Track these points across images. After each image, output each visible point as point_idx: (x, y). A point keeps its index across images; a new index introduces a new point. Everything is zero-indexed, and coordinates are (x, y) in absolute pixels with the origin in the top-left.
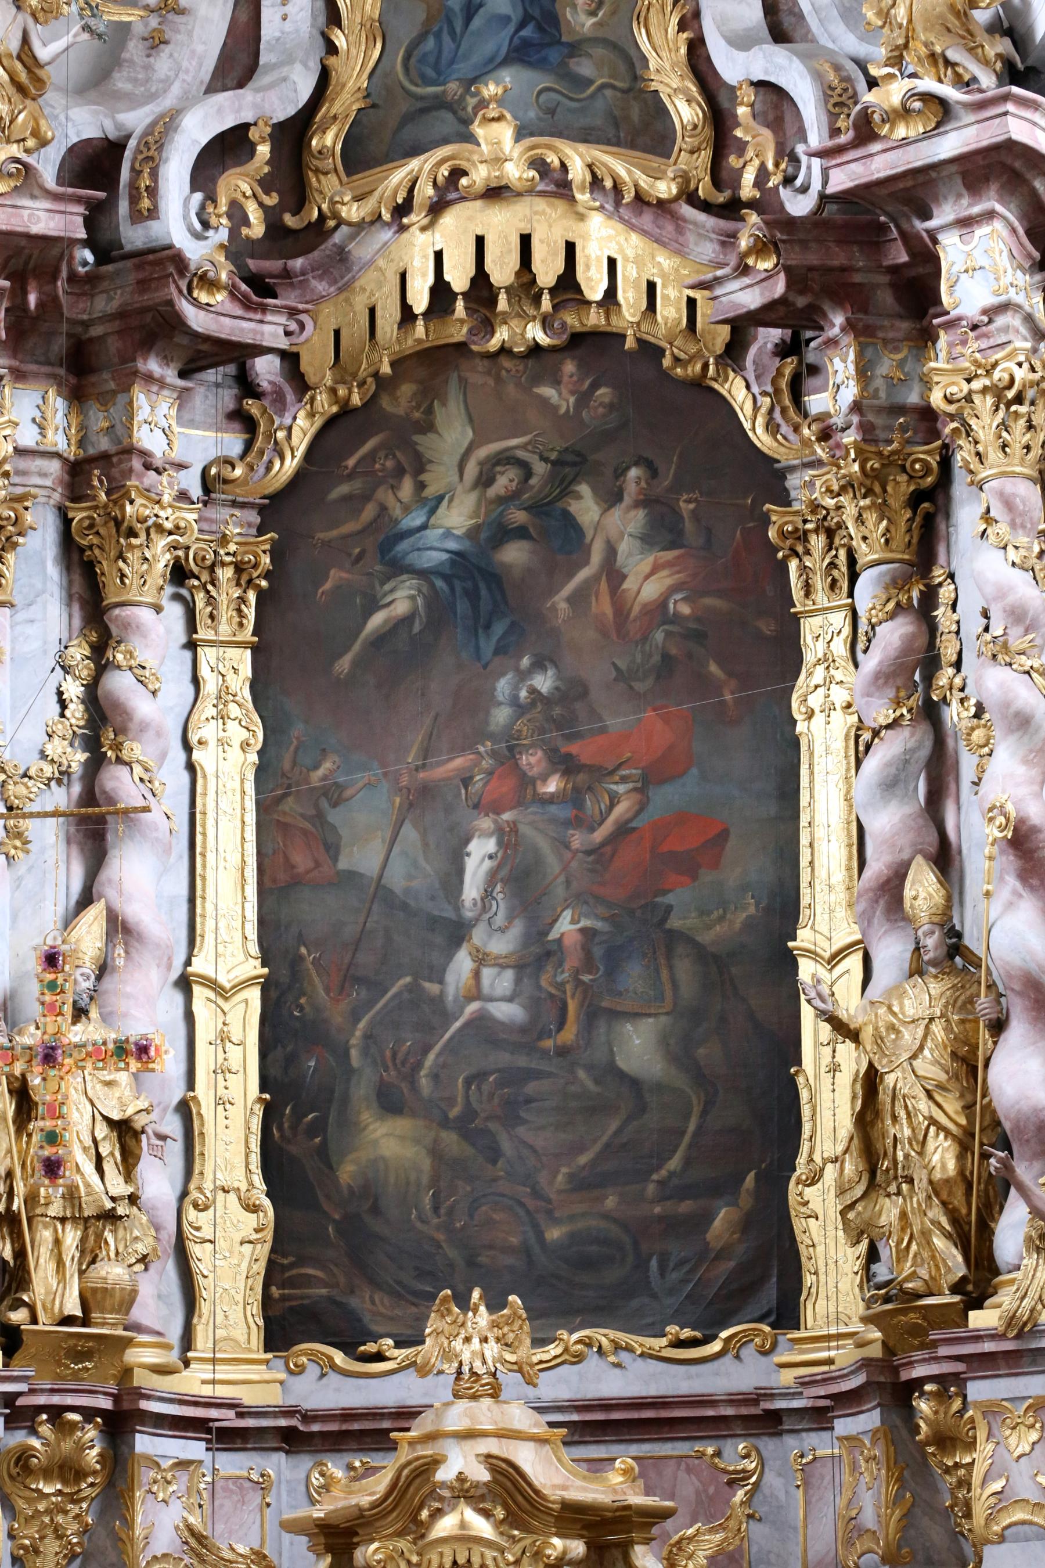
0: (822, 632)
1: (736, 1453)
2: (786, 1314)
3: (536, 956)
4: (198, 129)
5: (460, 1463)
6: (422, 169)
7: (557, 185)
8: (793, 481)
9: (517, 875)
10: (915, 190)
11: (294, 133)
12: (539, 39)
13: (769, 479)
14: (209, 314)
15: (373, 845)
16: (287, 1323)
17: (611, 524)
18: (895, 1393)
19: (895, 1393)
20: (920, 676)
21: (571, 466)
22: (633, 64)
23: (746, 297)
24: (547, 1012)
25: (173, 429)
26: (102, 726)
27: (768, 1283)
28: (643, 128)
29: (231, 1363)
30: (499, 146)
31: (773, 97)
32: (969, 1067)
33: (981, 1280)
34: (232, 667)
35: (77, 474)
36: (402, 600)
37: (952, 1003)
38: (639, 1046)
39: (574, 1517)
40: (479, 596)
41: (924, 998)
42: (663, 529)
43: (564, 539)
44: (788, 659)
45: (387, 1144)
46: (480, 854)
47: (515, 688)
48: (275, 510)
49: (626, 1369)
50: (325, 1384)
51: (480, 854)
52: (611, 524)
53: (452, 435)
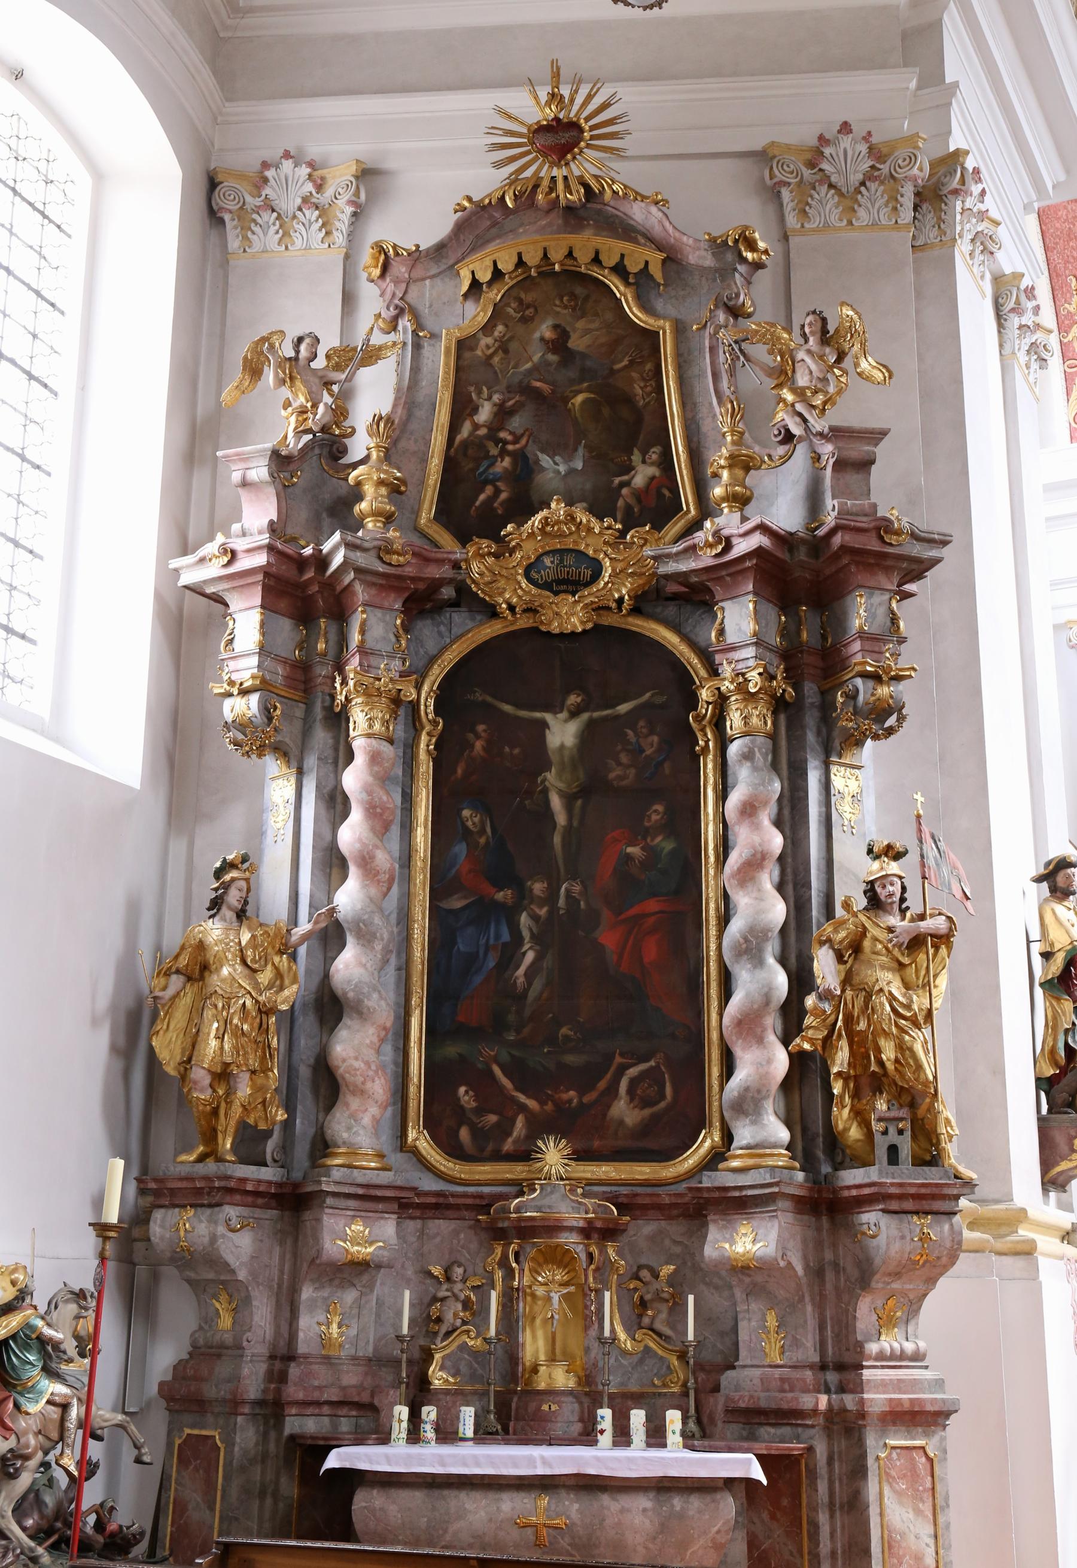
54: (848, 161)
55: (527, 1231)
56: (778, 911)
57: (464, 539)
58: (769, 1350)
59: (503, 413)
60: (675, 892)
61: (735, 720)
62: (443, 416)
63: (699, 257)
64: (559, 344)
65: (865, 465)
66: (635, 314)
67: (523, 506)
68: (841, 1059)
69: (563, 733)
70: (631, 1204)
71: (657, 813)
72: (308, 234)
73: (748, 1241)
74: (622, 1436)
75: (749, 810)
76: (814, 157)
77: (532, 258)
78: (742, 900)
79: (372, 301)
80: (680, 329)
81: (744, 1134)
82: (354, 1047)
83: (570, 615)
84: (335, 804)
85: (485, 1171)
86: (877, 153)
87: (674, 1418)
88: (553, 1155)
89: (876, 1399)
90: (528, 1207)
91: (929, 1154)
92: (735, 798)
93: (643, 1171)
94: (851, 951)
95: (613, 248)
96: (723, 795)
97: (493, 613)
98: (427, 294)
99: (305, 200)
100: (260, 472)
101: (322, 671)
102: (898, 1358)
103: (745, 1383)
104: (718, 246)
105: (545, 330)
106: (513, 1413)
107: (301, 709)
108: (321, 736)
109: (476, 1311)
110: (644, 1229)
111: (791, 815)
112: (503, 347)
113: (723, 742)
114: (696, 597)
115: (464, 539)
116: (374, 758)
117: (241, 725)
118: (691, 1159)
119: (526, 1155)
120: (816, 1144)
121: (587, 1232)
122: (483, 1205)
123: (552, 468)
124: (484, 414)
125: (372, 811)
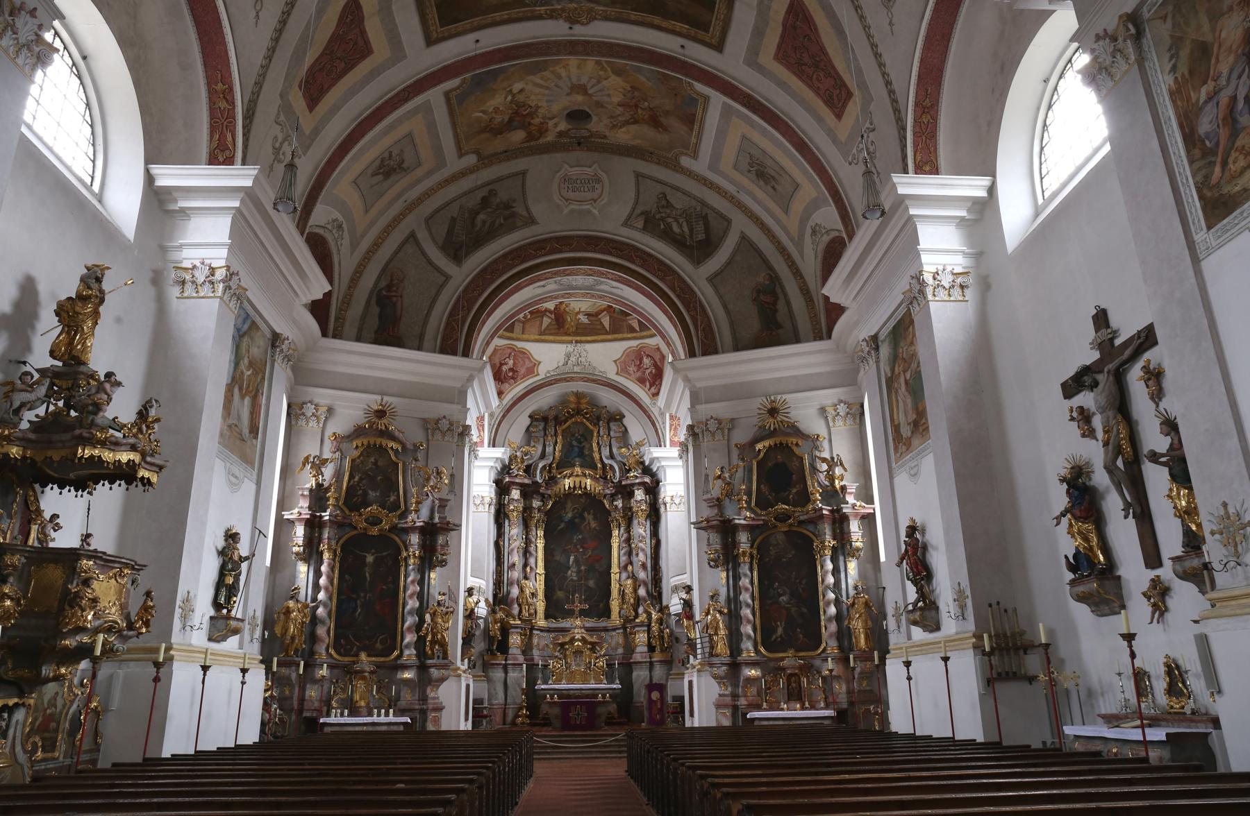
0: (615, 533)
1: (603, 634)
2: (609, 617)
3: (579, 572)
4: (541, 465)
5: (578, 637)
6: (568, 472)
7: (585, 475)
8: (613, 514)
9: (576, 561)
10: (633, 485)
11: (550, 465)
12: (581, 454)
13: (608, 513)
14: (542, 490)
15: (559, 557)
16: (547, 617)
17: (589, 517)
18: (625, 628)
19: (625, 628)
20: (628, 540)
21: (584, 510)
22: (593, 458)
23: (608, 492)
24: (580, 579)
25: (536, 503)
26: (528, 542)
27: (607, 613)
28: (594, 467)
29: (541, 622)
30: (578, 470)
31: (612, 467)
32: (635, 590)
33: (637, 616)
34: (541, 533)
35: (525, 509)
36: (563, 525)
37: (667, 607)
38: (591, 583)
39: (591, 643)
40: (573, 526)
41: (629, 582)
42: (595, 518)
43: (583, 519)
44: (611, 536)
45: (560, 594)
46: (572, 558)
47: (577, 537)
48: (547, 513)
49: (590, 623)
50: (553, 624)
51: (572, 558)
52: (589, 517)
53: (569, 505)
54: (444, 425)
55: (357, 672)
56: (417, 604)
57: (351, 510)
58: (407, 697)
59: (361, 479)
60: (392, 597)
61: (411, 561)
62: (346, 478)
63: (410, 446)
64: (375, 464)
65: (445, 506)
66: (393, 458)
67: (366, 504)
68: (429, 638)
69: (370, 559)
70: (379, 666)
71: (390, 579)
72: (313, 423)
73: (407, 675)
74: (379, 715)
75: (413, 582)
76: (437, 421)
77: (372, 442)
78: (410, 602)
79: (328, 446)
80: (404, 464)
81: (407, 652)
82: (321, 631)
83: (375, 531)
84: (318, 574)
85: (346, 659)
86: (451, 424)
87: (391, 711)
88: (363, 656)
89: (431, 706)
90: (357, 667)
91: (445, 656)
92: (410, 579)
93: (382, 659)
94: (433, 615)
95: (392, 444)
96: (406, 577)
97: (355, 528)
98: (344, 446)
99: (313, 414)
100: (306, 493)
101: (316, 541)
102: (434, 698)
103: (402, 704)
104: (415, 445)
105: (372, 460)
106: (353, 713)
107: (311, 552)
108: (314, 556)
109: (344, 690)
110: (381, 672)
111: (421, 582)
112: (362, 462)
113: (407, 566)
114: (407, 531)
115: (351, 510)
116: (329, 564)
117: (297, 554)
118: (392, 657)
119: (357, 655)
120: (421, 654)
121: (371, 672)
122: (346, 666)
123: (372, 494)
124: (357, 479)
125: (328, 577)
